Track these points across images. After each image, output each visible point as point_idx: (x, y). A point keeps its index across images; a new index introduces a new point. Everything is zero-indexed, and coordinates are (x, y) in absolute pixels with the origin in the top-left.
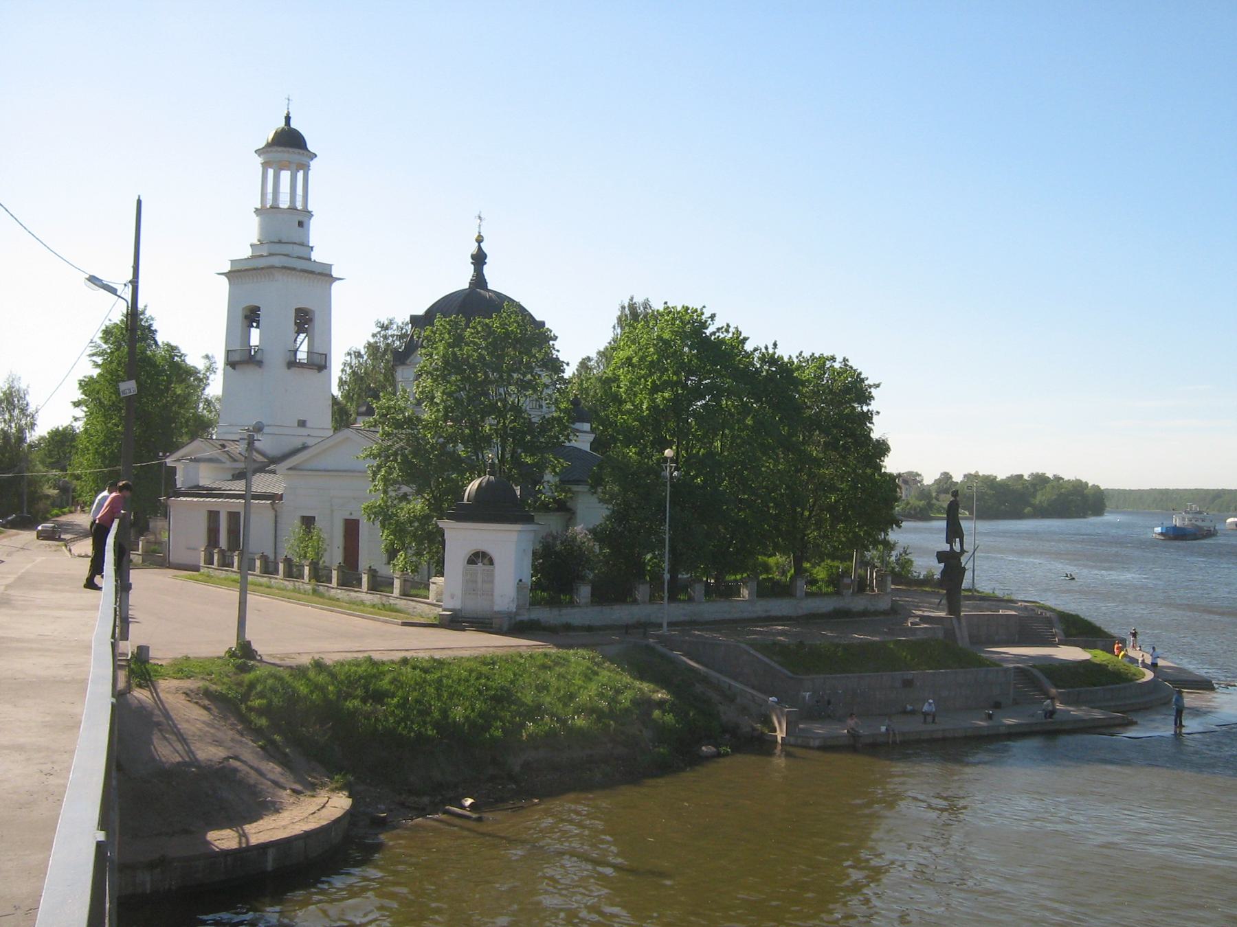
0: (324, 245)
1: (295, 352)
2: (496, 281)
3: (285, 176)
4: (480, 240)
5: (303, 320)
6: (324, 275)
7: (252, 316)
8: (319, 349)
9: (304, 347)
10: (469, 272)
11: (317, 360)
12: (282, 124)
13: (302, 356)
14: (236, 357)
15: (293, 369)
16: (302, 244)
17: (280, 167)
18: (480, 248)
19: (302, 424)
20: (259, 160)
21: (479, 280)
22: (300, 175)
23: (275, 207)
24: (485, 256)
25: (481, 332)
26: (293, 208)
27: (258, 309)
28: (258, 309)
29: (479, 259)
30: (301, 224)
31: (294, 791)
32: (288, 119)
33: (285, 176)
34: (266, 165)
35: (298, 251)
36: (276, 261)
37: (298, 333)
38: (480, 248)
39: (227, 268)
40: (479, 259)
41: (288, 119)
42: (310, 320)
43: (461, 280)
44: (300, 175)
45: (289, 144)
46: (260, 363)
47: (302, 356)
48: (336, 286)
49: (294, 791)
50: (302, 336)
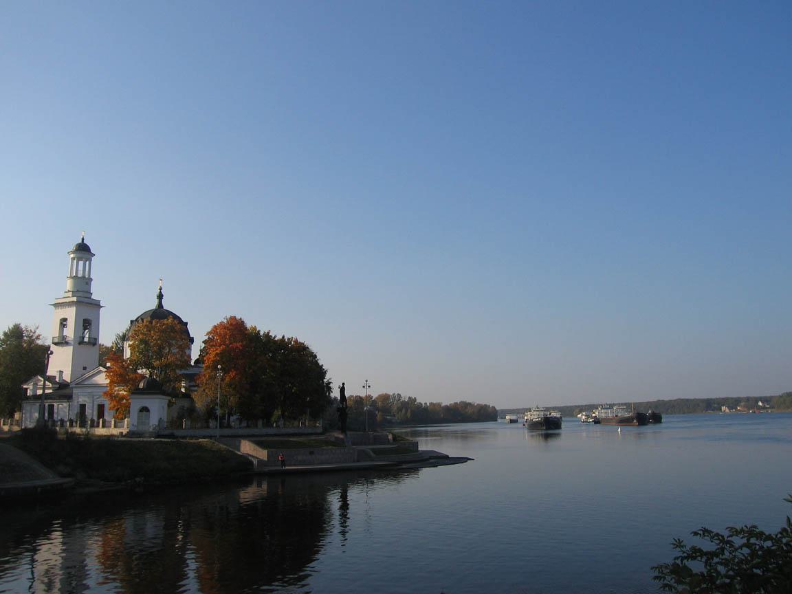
0: (97, 293)
1: (84, 337)
2: (167, 306)
3: (81, 263)
4: (161, 289)
6: (97, 305)
7: (63, 323)
8: (93, 336)
9: (87, 336)
10: (157, 301)
11: (92, 341)
12: (80, 241)
13: (86, 340)
14: (56, 340)
17: (79, 259)
18: (160, 292)
22: (87, 263)
24: (163, 296)
25: (162, 328)
26: (84, 277)
29: (160, 297)
31: (80, 528)
32: (83, 239)
33: (81, 263)
35: (86, 295)
37: (85, 330)
38: (160, 292)
40: (160, 297)
41: (83, 239)
42: (90, 324)
43: (153, 305)
44: (87, 263)
47: (86, 340)
49: (80, 528)
50: (87, 331)
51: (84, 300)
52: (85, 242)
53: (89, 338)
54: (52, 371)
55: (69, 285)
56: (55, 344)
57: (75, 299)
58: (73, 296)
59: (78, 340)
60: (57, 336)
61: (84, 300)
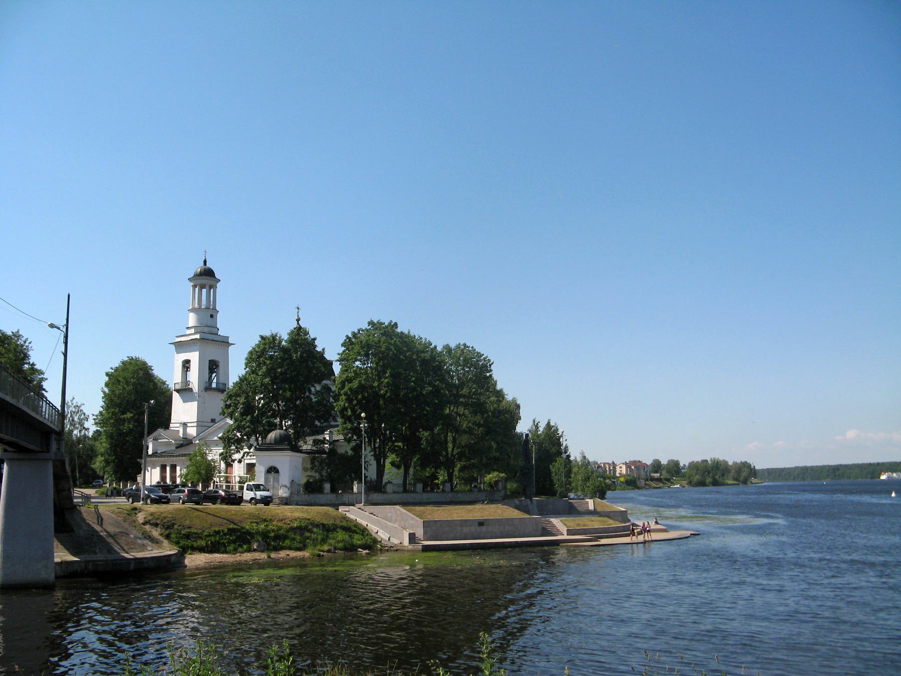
0: (224, 328)
3: (204, 291)
6: (225, 343)
7: (186, 364)
8: (221, 381)
9: (215, 381)
11: (221, 386)
14: (178, 387)
15: (210, 392)
17: (202, 287)
30: (212, 316)
32: (205, 262)
34: (195, 286)
42: (217, 366)
45: (206, 277)
47: (214, 385)
48: (231, 348)
51: (210, 338)
52: (208, 265)
53: (217, 383)
55: (192, 319)
56: (178, 391)
57: (198, 336)
58: (195, 333)
59: (204, 385)
60: (180, 381)
61: (210, 338)
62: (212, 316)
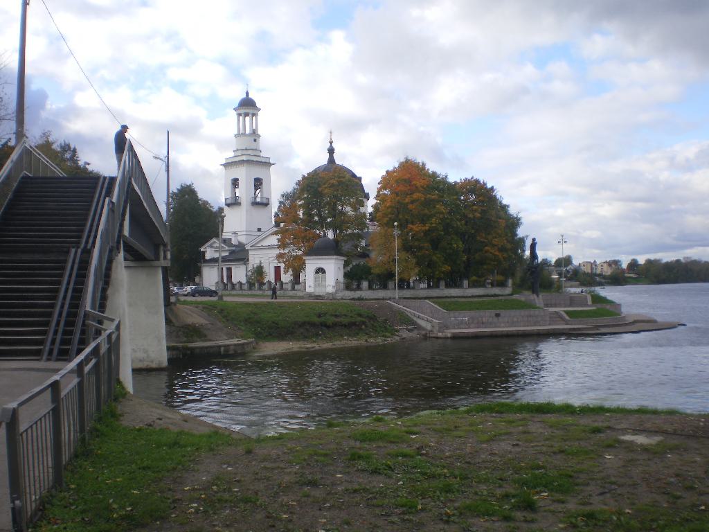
3: (248, 119)
4: (331, 143)
5: (258, 183)
7: (235, 183)
9: (259, 196)
10: (327, 156)
11: (265, 201)
12: (245, 96)
14: (229, 202)
16: (256, 150)
17: (246, 115)
19: (259, 230)
20: (234, 114)
21: (331, 160)
23: (244, 134)
27: (238, 179)
28: (238, 179)
30: (255, 140)
32: (247, 94)
34: (239, 115)
36: (244, 158)
37: (256, 189)
39: (224, 162)
40: (331, 151)
41: (247, 94)
42: (261, 184)
46: (239, 204)
53: (261, 198)
54: (226, 234)
56: (228, 205)
62: (255, 140)
